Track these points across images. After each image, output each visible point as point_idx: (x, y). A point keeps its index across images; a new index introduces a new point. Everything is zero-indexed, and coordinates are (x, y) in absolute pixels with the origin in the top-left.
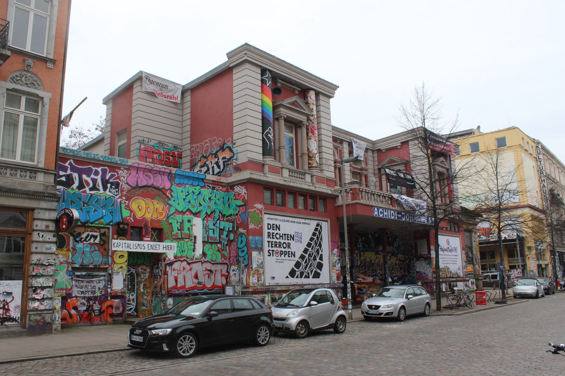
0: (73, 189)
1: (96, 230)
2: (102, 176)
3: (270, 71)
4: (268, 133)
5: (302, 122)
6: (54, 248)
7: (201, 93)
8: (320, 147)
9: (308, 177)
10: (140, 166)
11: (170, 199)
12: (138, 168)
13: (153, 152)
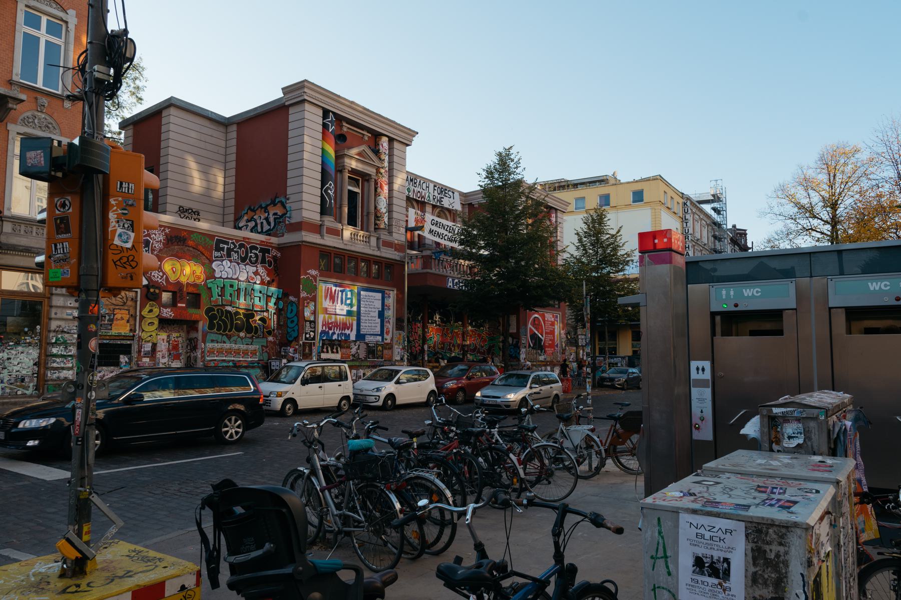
3: (333, 113)
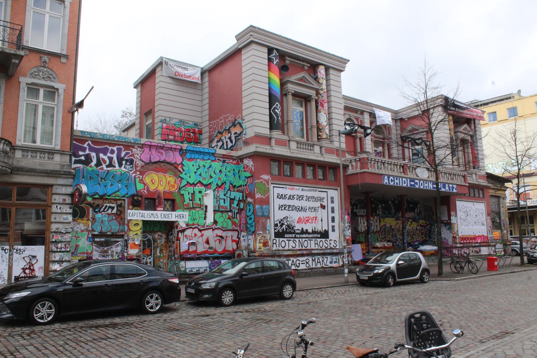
0: (91, 167)
1: (113, 201)
3: (277, 50)
4: (275, 108)
6: (70, 218)
8: (330, 119)
9: (317, 149)
10: (152, 144)
11: (181, 173)
12: (150, 146)
13: (174, 130)
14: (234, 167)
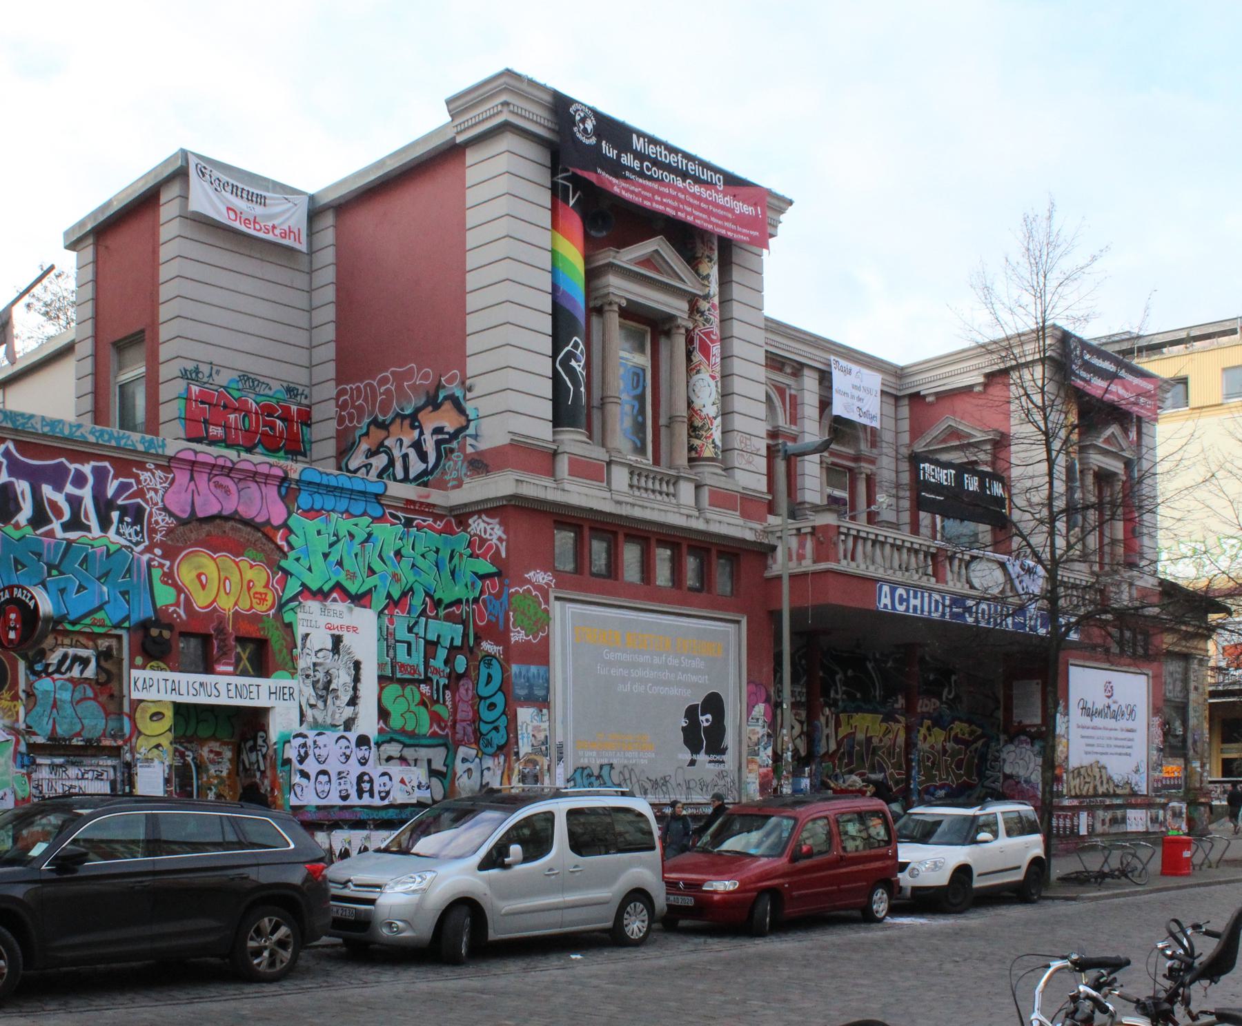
0: (17, 526)
2: (94, 488)
4: (570, 355)
5: (672, 318)
7: (366, 220)
8: (725, 395)
9: (686, 491)
10: (201, 458)
11: (285, 556)
12: (193, 463)
13: (225, 407)
14: (437, 539)
